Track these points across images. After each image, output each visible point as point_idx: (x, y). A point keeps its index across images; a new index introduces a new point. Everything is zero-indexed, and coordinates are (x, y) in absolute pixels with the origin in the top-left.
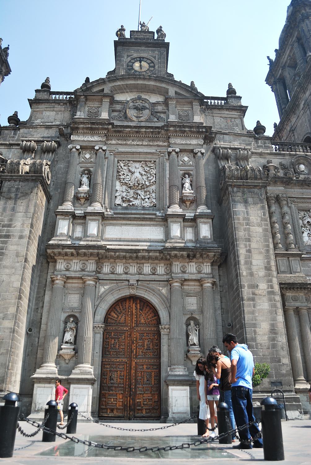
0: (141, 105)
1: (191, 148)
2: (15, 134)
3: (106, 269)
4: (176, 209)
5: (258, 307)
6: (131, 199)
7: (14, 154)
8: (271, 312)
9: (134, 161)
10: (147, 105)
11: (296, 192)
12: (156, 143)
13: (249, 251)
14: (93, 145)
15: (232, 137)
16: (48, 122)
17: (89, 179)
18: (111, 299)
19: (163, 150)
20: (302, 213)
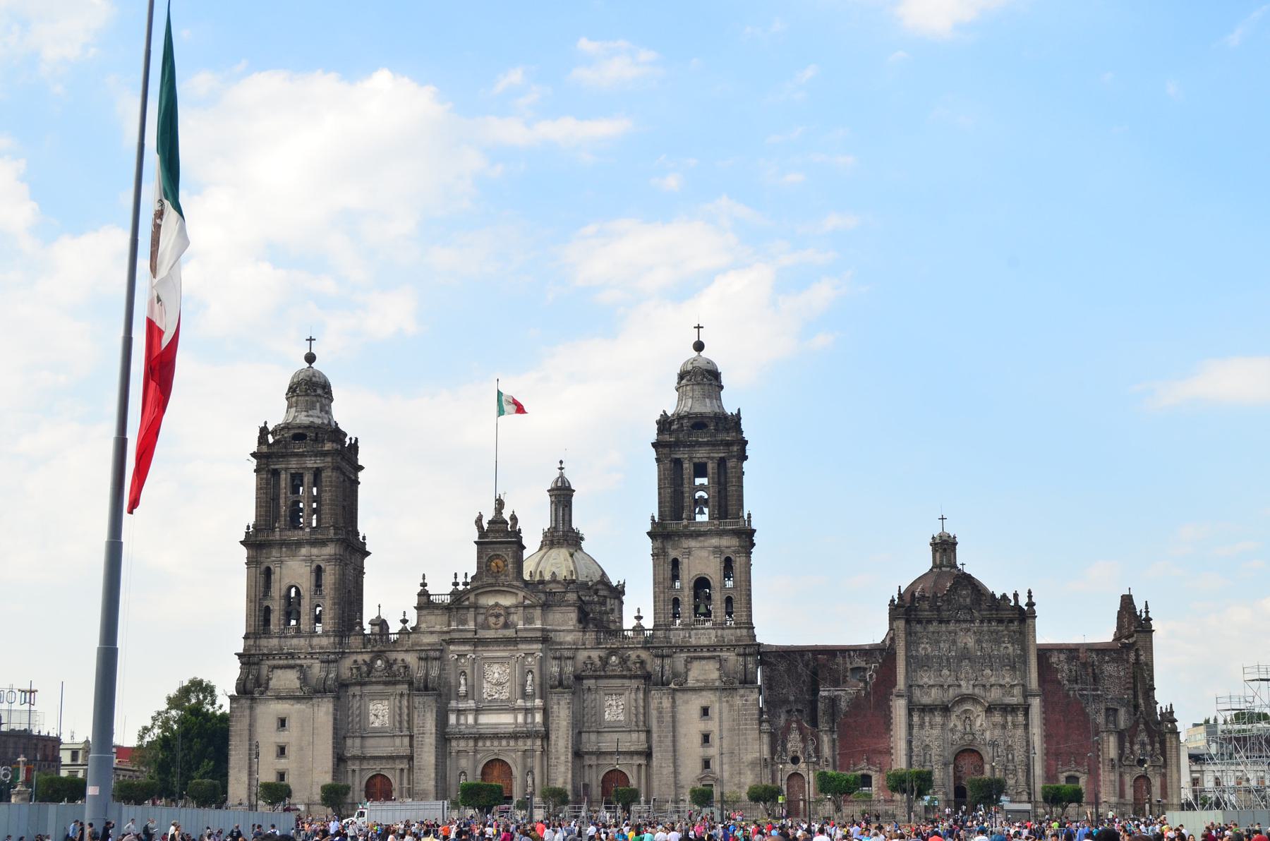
0: (498, 612)
2: (409, 638)
3: (480, 744)
4: (520, 702)
5: (559, 770)
6: (494, 694)
7: (412, 658)
8: (565, 773)
10: (502, 612)
11: (602, 683)
12: (509, 648)
13: (557, 737)
15: (565, 633)
17: (466, 679)
18: (485, 762)
19: (514, 653)
20: (607, 698)
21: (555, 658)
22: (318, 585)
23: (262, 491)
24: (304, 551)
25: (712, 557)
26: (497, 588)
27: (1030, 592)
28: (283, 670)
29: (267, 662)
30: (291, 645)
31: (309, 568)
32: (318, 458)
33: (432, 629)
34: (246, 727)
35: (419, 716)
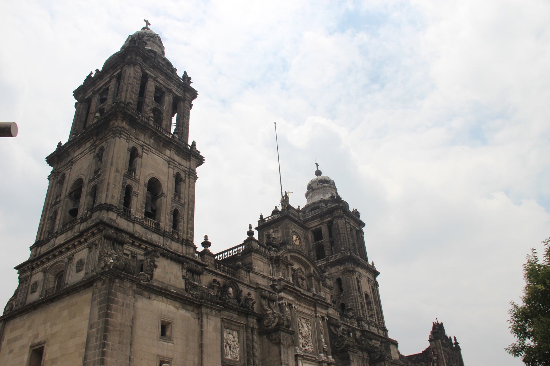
1: (323, 315)
2: (247, 275)
4: (323, 356)
9: (303, 318)
10: (303, 276)
14: (291, 303)
16: (263, 272)
19: (313, 313)
21: (333, 325)
22: (177, 192)
23: (135, 80)
24: (168, 152)
25: (368, 283)
26: (300, 257)
27: (455, 338)
28: (169, 261)
29: (131, 248)
30: (151, 239)
31: (171, 170)
32: (179, 89)
33: (262, 273)
34: (129, 324)
35: (284, 353)
